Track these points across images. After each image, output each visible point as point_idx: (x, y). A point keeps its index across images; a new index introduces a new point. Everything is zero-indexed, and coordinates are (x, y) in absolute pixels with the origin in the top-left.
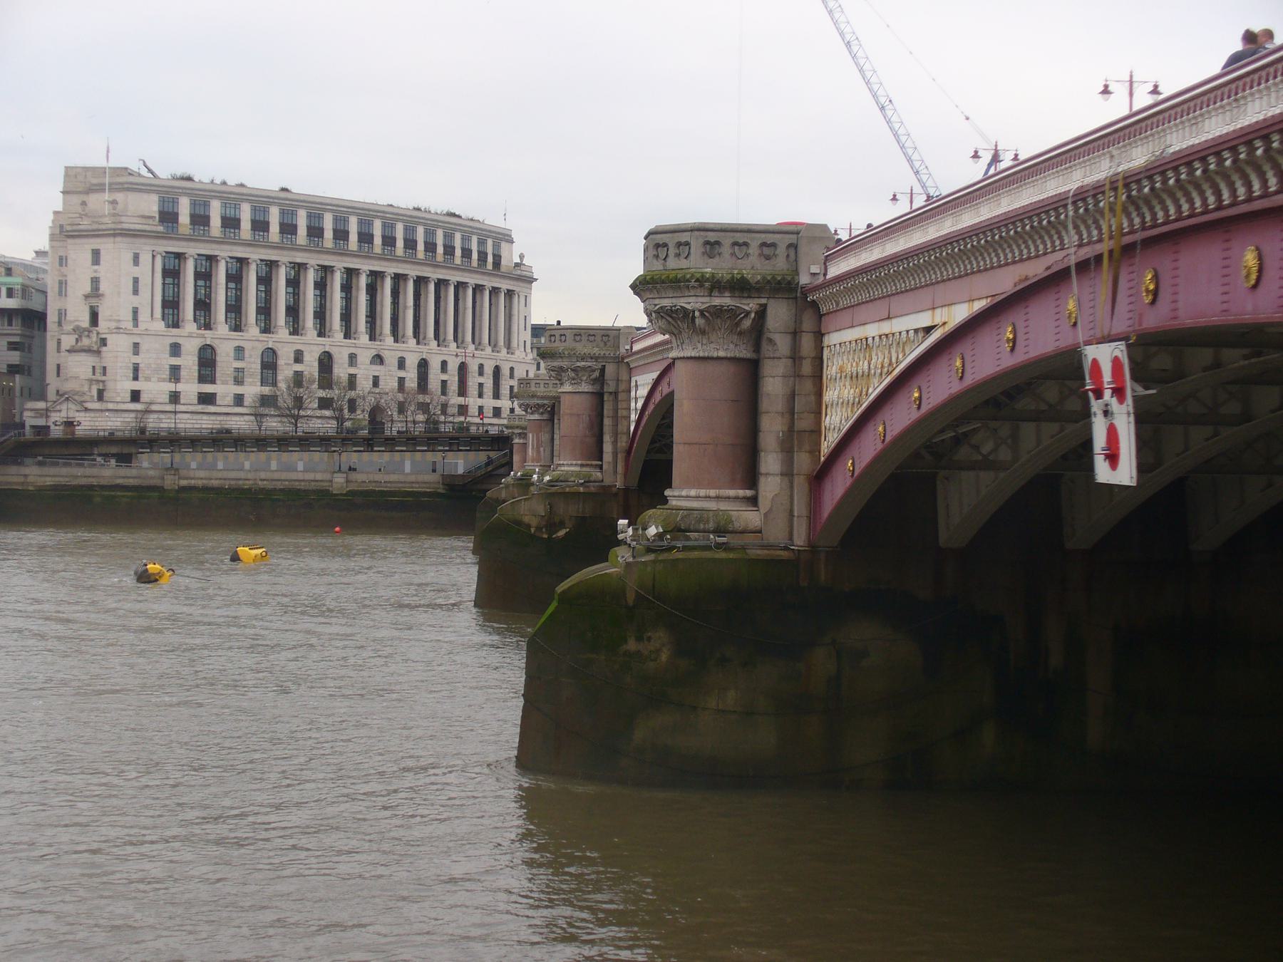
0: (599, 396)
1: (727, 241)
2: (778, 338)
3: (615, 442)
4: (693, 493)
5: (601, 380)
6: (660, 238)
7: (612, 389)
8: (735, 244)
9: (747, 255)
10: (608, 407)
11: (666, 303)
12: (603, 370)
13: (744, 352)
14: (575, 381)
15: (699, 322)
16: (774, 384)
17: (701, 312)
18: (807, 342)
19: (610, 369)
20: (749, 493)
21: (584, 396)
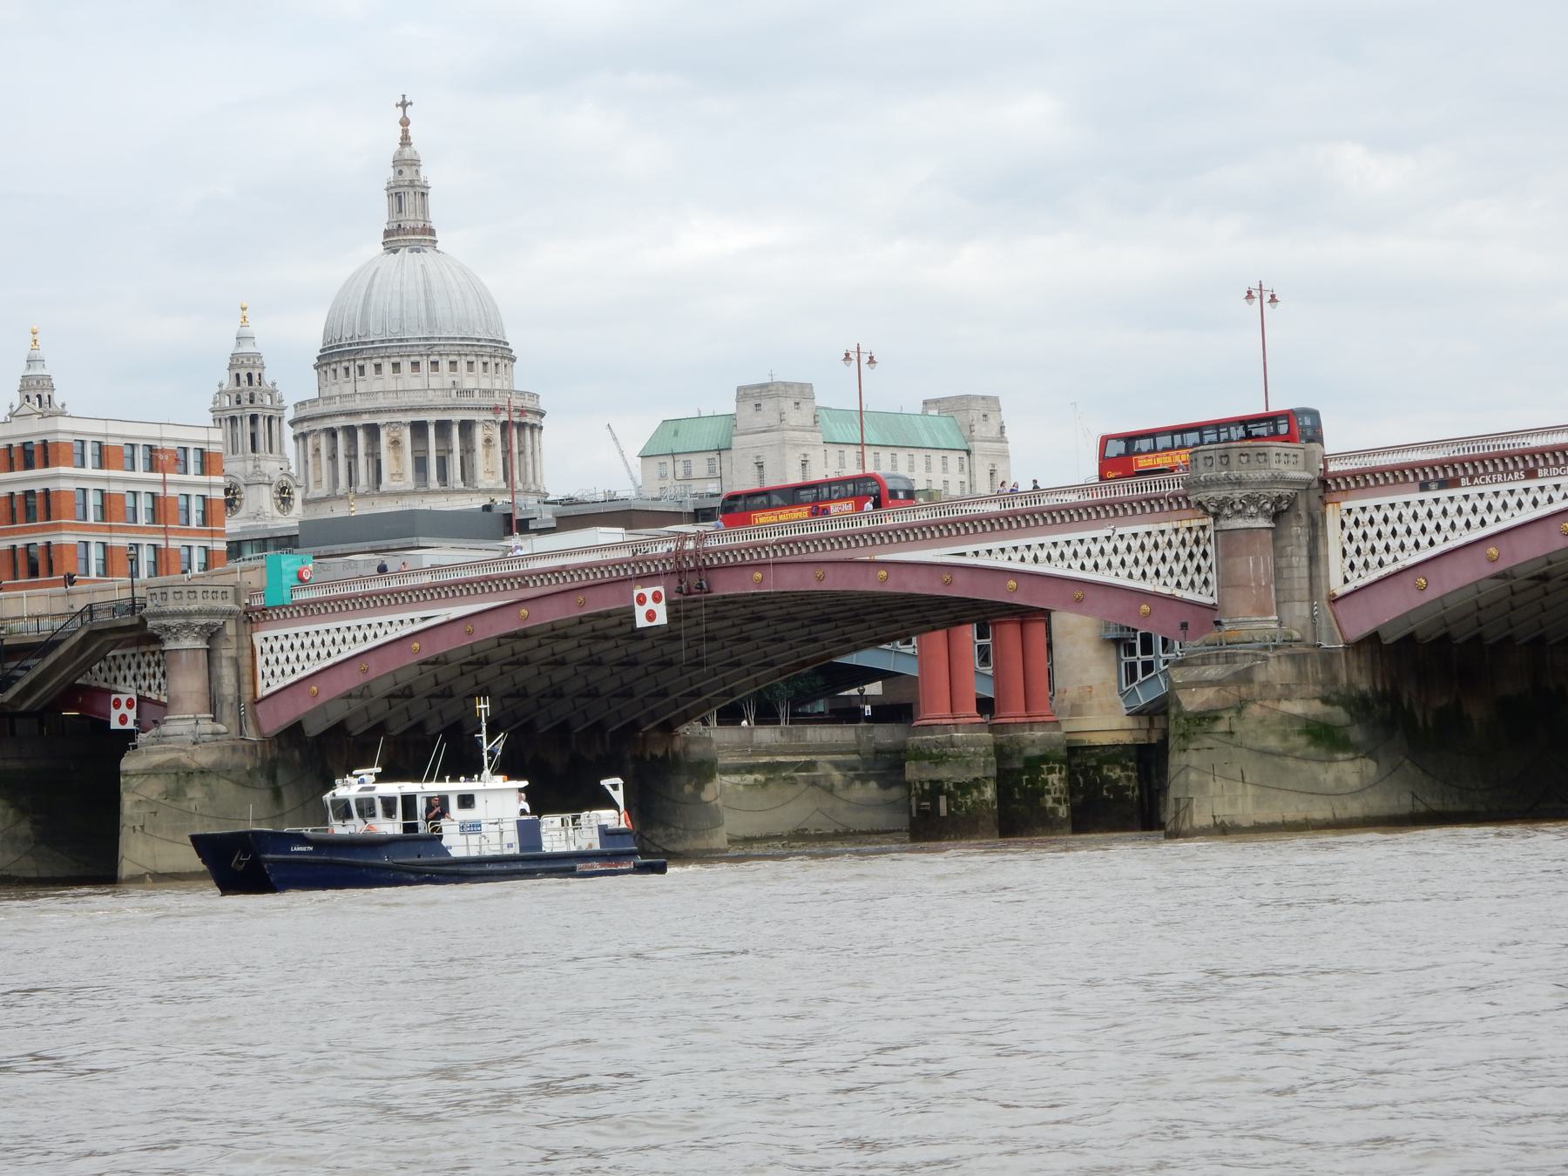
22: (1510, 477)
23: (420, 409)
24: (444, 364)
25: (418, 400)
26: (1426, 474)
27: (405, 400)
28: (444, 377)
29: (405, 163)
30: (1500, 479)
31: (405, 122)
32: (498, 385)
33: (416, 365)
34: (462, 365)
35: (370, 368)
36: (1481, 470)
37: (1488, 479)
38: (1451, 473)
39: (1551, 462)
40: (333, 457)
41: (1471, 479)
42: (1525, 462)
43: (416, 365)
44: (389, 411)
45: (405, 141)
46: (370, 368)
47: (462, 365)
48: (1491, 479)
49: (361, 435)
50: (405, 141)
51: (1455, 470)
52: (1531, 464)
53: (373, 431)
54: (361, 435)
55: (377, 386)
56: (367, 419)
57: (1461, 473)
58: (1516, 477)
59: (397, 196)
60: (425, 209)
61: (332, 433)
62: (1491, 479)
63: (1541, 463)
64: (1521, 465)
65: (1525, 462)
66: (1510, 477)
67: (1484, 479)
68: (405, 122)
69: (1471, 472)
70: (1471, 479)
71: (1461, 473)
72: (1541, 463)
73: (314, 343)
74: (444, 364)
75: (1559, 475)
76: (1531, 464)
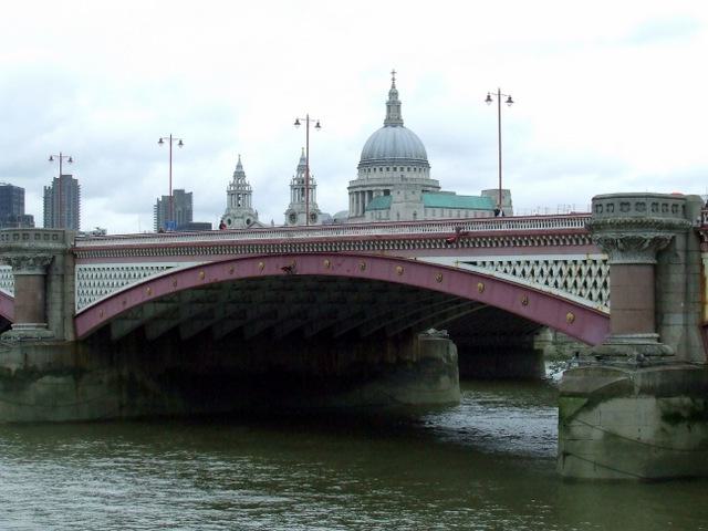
0: (46, 279)
1: (615, 201)
2: (679, 253)
3: (62, 309)
4: (640, 335)
5: (47, 268)
6: (597, 202)
7: (60, 272)
8: (637, 204)
9: (629, 210)
10: (55, 285)
11: (630, 235)
12: (54, 258)
13: (655, 262)
14: (32, 267)
15: (620, 245)
16: (677, 277)
17: (621, 240)
18: (695, 256)
19: (59, 259)
20: (656, 335)
21: (37, 278)
23: (387, 185)
24: (398, 169)
25: (386, 182)
27: (382, 182)
28: (398, 174)
29: (393, 94)
31: (393, 79)
32: (420, 176)
33: (388, 169)
34: (406, 169)
35: (372, 170)
40: (358, 202)
43: (388, 169)
44: (378, 185)
45: (393, 87)
46: (372, 170)
47: (406, 169)
49: (367, 194)
50: (393, 87)
53: (370, 192)
54: (367, 194)
55: (375, 176)
56: (368, 189)
59: (389, 105)
60: (399, 111)
61: (363, 192)
68: (393, 79)
73: (358, 160)
74: (398, 169)
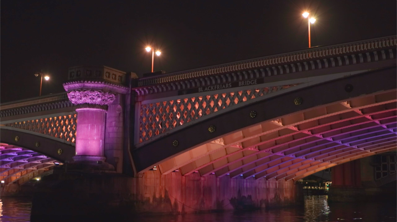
22: (224, 86)
26: (181, 86)
30: (218, 88)
36: (209, 83)
37: (212, 88)
38: (193, 85)
39: (246, 77)
41: (204, 89)
42: (232, 77)
48: (214, 88)
51: (196, 83)
52: (235, 79)
57: (198, 84)
58: (227, 86)
62: (214, 88)
63: (241, 78)
64: (230, 80)
65: (232, 77)
66: (224, 86)
67: (210, 88)
69: (203, 84)
70: (204, 89)
71: (198, 84)
72: (241, 78)
75: (250, 84)
76: (235, 79)
